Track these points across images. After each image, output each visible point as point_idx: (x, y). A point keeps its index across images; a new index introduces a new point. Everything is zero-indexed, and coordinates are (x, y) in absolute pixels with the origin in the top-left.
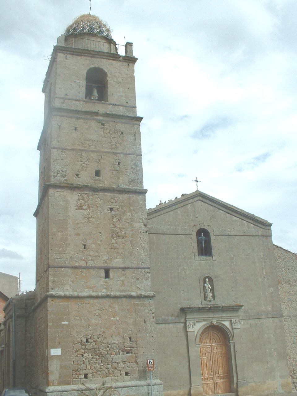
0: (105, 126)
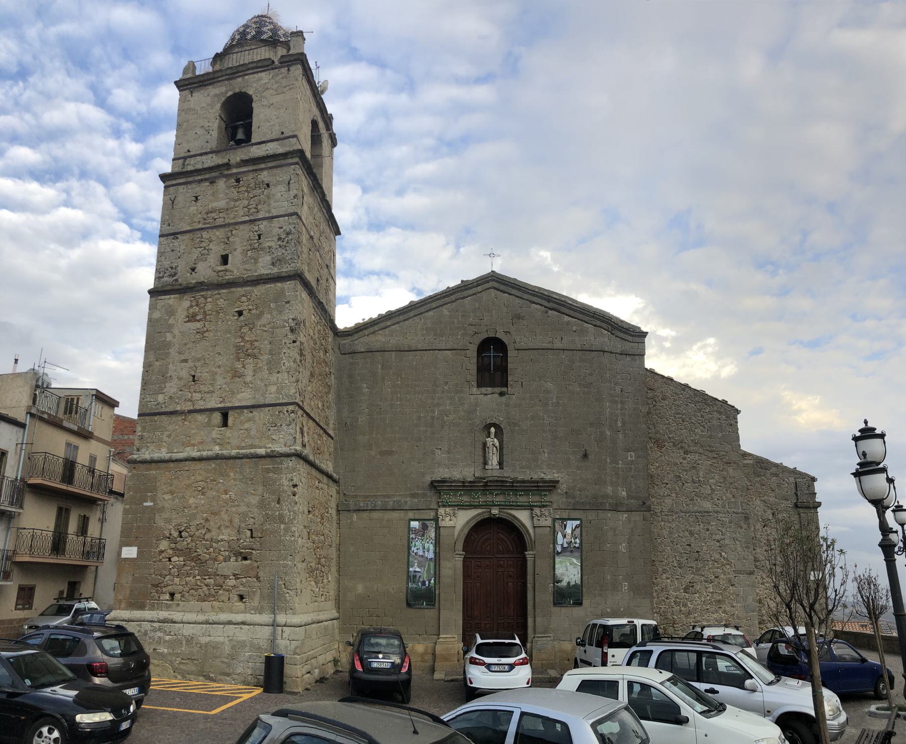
0: (241, 182)
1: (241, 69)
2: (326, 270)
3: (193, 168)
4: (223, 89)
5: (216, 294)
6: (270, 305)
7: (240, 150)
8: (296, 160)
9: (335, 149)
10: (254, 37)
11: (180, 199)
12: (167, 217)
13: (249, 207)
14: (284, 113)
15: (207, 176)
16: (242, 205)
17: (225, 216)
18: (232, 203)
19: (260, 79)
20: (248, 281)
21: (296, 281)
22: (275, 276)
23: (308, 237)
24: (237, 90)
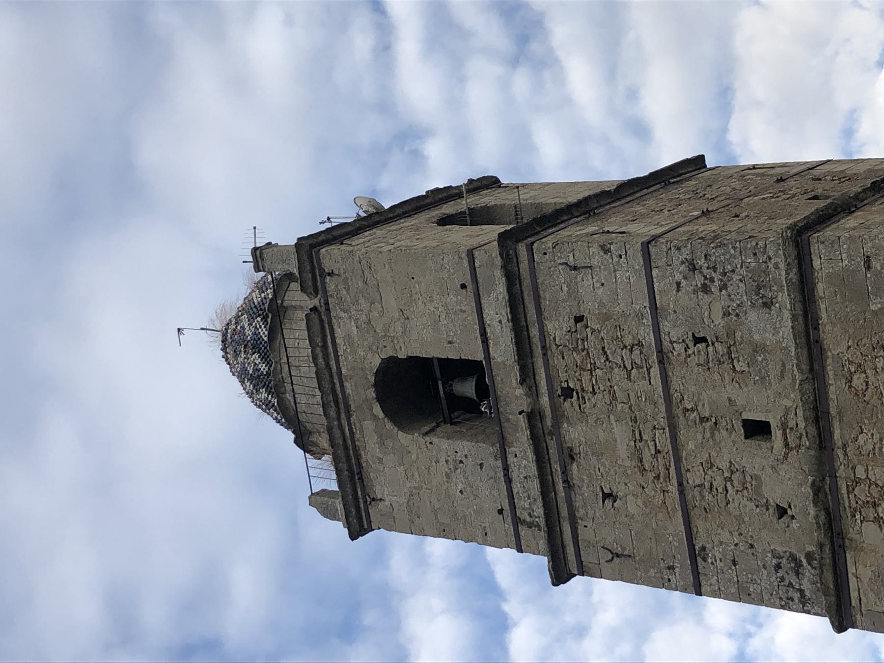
0: (571, 385)
1: (327, 386)
2: (791, 182)
3: (540, 503)
4: (369, 425)
5: (846, 454)
6: (875, 313)
7: (499, 386)
8: (522, 248)
9: (504, 181)
10: (265, 358)
11: (609, 536)
12: (652, 572)
13: (629, 367)
14: (419, 283)
15: (557, 467)
16: (625, 384)
17: (649, 425)
18: (619, 407)
19: (348, 337)
20: (811, 370)
21: (813, 240)
22: (799, 298)
23: (703, 220)
24: (372, 393)
